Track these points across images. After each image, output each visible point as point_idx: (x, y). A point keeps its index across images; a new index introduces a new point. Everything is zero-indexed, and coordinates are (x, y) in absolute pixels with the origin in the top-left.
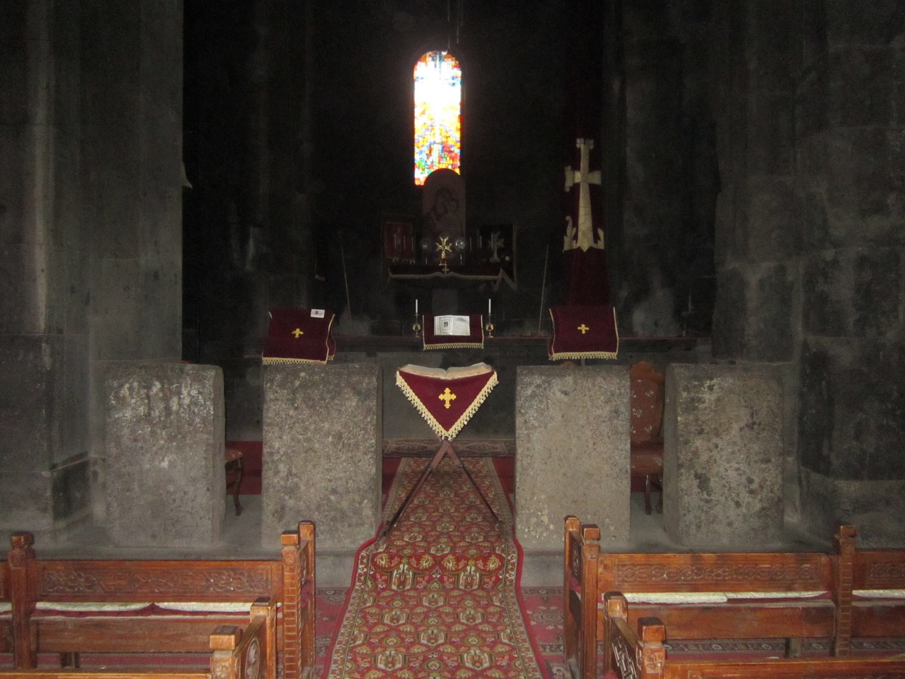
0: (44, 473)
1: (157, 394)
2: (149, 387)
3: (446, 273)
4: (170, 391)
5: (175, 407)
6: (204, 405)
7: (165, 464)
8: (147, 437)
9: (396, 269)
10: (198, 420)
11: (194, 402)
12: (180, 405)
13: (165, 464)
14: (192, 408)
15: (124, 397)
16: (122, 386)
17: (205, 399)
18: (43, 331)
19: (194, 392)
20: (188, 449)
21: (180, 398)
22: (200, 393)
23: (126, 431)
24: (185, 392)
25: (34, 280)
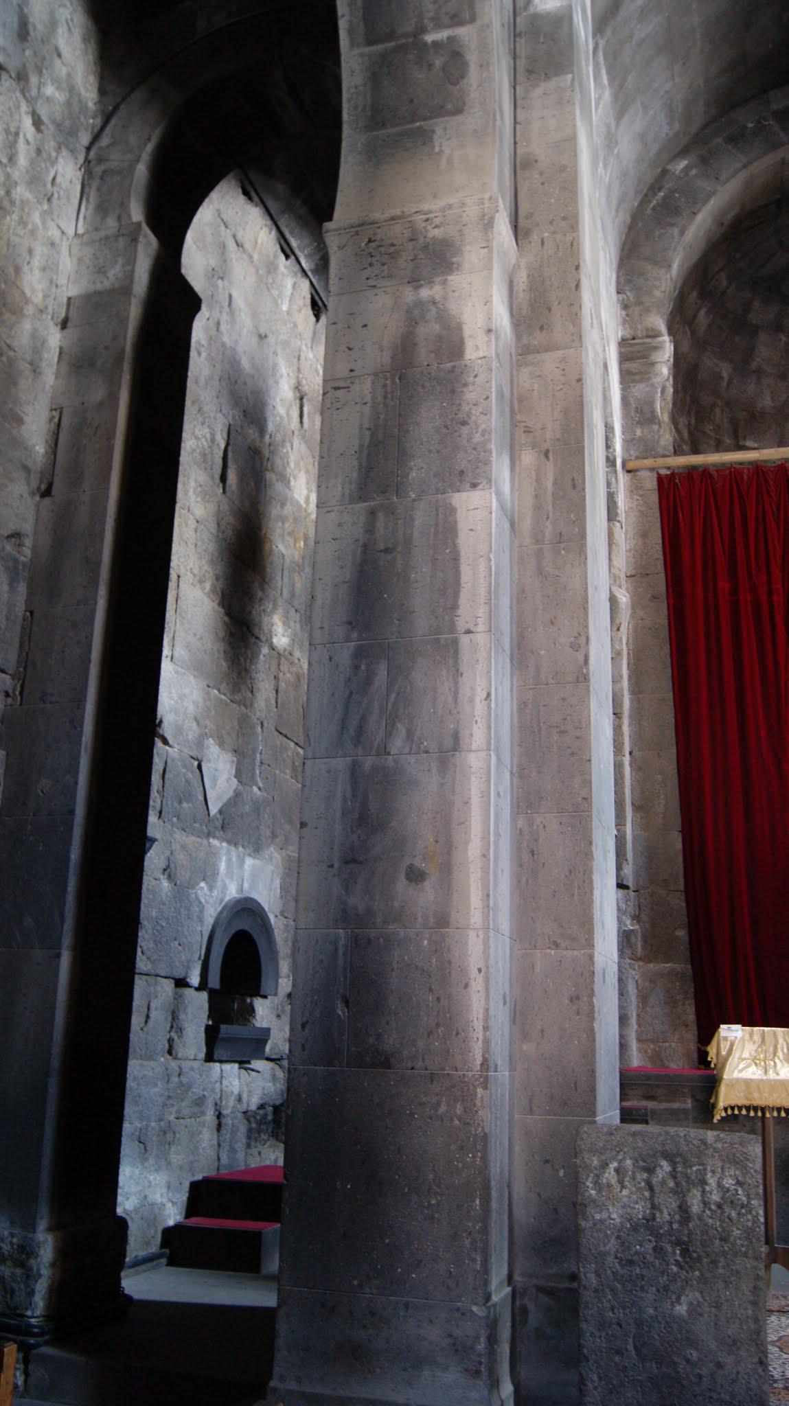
0: (475, 1308)
1: (663, 1183)
2: (650, 1170)
4: (688, 1177)
5: (696, 1208)
6: (748, 1207)
7: (682, 1309)
8: (650, 1258)
10: (736, 1232)
12: (705, 1204)
13: (682, 1309)
14: (727, 1209)
15: (609, 1186)
16: (605, 1165)
17: (748, 1196)
18: (479, 1068)
19: (728, 1182)
20: (720, 1285)
21: (704, 1191)
22: (739, 1183)
23: (612, 1245)
24: (712, 1181)
25: (466, 986)
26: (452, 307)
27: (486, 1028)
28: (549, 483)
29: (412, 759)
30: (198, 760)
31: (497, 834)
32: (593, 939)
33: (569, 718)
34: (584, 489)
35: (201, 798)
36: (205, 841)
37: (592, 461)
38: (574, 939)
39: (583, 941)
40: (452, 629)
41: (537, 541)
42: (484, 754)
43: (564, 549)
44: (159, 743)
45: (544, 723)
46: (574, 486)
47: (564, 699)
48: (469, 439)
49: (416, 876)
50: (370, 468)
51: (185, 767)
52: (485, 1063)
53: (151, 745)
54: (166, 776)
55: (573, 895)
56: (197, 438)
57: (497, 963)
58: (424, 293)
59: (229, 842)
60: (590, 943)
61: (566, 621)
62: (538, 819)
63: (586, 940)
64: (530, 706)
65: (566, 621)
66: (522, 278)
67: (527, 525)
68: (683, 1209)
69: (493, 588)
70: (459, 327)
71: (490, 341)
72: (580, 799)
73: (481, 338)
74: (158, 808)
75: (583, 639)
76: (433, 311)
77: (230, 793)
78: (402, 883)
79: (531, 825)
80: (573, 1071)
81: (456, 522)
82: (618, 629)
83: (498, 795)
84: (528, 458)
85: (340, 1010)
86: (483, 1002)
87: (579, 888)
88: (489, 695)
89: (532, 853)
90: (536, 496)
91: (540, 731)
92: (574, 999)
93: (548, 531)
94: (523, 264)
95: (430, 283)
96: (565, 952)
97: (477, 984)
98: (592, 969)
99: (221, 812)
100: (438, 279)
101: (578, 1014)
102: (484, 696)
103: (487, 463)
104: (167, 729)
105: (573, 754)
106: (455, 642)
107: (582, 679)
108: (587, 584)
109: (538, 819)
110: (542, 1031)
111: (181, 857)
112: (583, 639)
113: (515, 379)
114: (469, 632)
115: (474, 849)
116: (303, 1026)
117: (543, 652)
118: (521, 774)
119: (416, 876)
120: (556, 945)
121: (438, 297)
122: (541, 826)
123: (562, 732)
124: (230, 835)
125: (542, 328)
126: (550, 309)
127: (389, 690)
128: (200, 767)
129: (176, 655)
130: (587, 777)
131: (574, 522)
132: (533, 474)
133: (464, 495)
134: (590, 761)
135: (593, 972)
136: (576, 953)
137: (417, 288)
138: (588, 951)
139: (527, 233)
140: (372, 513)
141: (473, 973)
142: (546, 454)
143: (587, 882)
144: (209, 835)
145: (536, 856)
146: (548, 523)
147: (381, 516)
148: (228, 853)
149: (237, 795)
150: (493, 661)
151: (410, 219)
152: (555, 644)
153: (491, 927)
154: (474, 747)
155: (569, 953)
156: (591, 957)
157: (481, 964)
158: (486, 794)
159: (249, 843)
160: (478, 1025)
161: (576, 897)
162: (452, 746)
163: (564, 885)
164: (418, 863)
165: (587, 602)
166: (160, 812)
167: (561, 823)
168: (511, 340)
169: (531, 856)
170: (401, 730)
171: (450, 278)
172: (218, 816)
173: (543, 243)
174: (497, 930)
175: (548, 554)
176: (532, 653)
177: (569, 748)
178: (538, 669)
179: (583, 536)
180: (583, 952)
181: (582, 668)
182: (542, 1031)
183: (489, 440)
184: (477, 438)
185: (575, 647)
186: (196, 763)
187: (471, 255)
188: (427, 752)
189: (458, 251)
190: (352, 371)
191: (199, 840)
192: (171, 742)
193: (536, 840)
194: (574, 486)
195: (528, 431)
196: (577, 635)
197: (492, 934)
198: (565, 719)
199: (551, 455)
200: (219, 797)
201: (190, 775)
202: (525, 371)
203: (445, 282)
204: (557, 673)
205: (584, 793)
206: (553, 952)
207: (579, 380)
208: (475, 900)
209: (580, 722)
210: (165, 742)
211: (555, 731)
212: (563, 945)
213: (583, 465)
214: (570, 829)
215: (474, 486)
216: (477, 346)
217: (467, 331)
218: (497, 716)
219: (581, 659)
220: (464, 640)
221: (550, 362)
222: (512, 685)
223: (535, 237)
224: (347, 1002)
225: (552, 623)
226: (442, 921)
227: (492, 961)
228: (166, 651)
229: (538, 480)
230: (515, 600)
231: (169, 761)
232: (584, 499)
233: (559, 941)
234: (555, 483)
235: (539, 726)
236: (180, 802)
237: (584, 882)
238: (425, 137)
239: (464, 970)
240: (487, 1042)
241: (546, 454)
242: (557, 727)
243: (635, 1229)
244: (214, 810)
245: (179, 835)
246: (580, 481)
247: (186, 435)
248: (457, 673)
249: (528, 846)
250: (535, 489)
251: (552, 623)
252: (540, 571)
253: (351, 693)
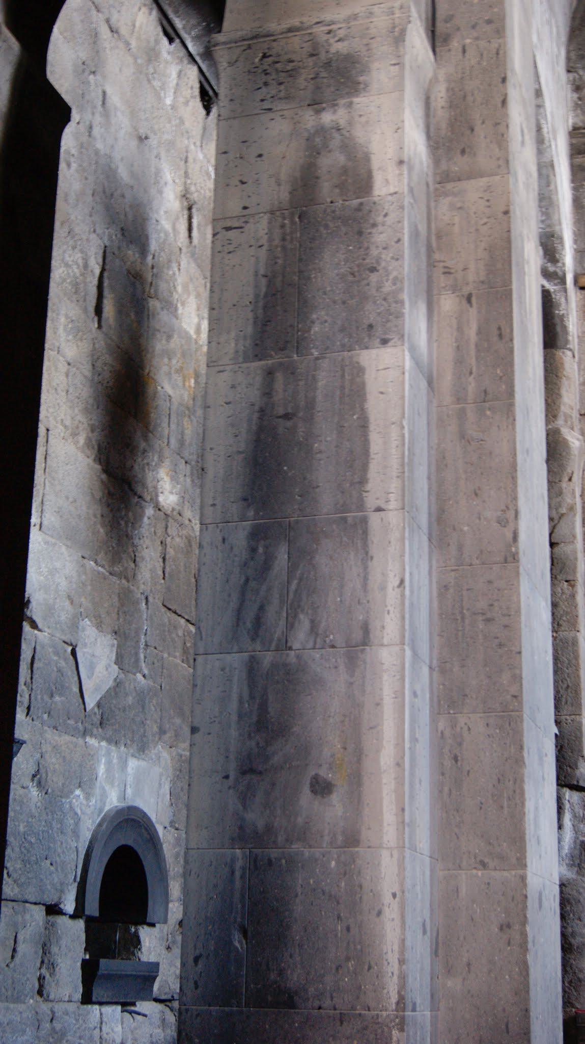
18: (394, 1007)
25: (379, 913)
26: (359, 134)
27: (402, 962)
28: (472, 332)
29: (317, 655)
30: (71, 645)
31: (414, 740)
32: (525, 858)
33: (496, 604)
34: (512, 340)
35: (76, 689)
36: (81, 741)
37: (522, 303)
38: (502, 858)
39: (514, 861)
40: (361, 506)
41: (458, 400)
42: (397, 649)
43: (489, 409)
44: (26, 627)
45: (468, 609)
46: (500, 336)
47: (490, 582)
48: (378, 289)
49: (321, 788)
50: (266, 322)
51: (57, 653)
52: (401, 1002)
53: (20, 628)
54: (35, 666)
55: (502, 807)
56: (67, 265)
57: (414, 886)
58: (327, 118)
59: (109, 741)
60: (521, 863)
61: (492, 493)
62: (462, 720)
63: (518, 859)
64: (451, 591)
65: (492, 493)
66: (440, 95)
67: (447, 381)
70: (367, 158)
71: (401, 174)
72: (509, 697)
73: (392, 171)
74: (26, 705)
75: (511, 514)
77: (110, 683)
78: (306, 796)
79: (453, 726)
80: (504, 1010)
81: (364, 384)
82: (570, 480)
83: (415, 694)
84: (448, 303)
85: (238, 941)
86: (398, 930)
87: (509, 799)
88: (402, 582)
89: (456, 759)
90: (458, 347)
91: (463, 618)
92: (505, 927)
93: (472, 388)
94: (441, 76)
96: (493, 873)
97: (391, 912)
98: (525, 892)
99: (99, 705)
100: (342, 102)
101: (509, 944)
103: (399, 315)
104: (35, 610)
105: (500, 645)
106: (364, 521)
107: (510, 559)
108: (515, 449)
109: (462, 720)
110: (469, 965)
111: (52, 761)
112: (511, 514)
113: (433, 212)
114: (379, 509)
115: (386, 757)
116: (196, 960)
117: (466, 528)
118: (442, 668)
119: (321, 788)
120: (484, 865)
121: (342, 123)
122: (466, 728)
123: (488, 620)
124: (110, 733)
125: (463, 152)
126: (472, 130)
127: (291, 572)
128: (74, 653)
129: (45, 523)
130: (517, 672)
131: (501, 377)
132: (454, 322)
133: (374, 352)
134: (520, 653)
135: (526, 897)
136: (506, 874)
137: (318, 112)
138: (520, 872)
139: (447, 39)
140: (270, 373)
141: (387, 898)
142: (469, 299)
143: (518, 792)
144: (85, 733)
145: (459, 764)
146: (471, 379)
147: (279, 377)
148: (108, 753)
149: (118, 684)
150: (407, 542)
151: (309, 31)
152: (480, 519)
153: (407, 845)
154: (385, 641)
155: (497, 874)
156: (523, 879)
157: (396, 888)
158: (399, 695)
159: (132, 741)
160: (393, 958)
161: (506, 810)
163: (493, 796)
164: (323, 773)
165: (516, 471)
166: (29, 708)
167: (487, 725)
168: (428, 167)
169: (454, 762)
170: (304, 621)
171: (356, 100)
172: (96, 710)
173: (464, 51)
174: (413, 848)
175: (471, 415)
176: (454, 529)
177: (497, 638)
178: (460, 548)
179: (511, 393)
180: (513, 872)
181: (511, 546)
182: (469, 965)
183: (401, 290)
184: (388, 287)
185: (502, 522)
186: (70, 648)
188: (333, 647)
189: (365, 70)
190: (245, 208)
191: (74, 739)
192: (40, 626)
193: (460, 744)
194: (500, 336)
195: (447, 272)
196: (504, 508)
197: (408, 853)
198: (492, 605)
199: (474, 300)
200: (96, 689)
201: (63, 664)
202: (445, 202)
203: (350, 104)
204: (481, 552)
205: (513, 690)
206: (480, 873)
207: (506, 213)
208: (389, 816)
209: (508, 608)
210: (34, 625)
211: (480, 618)
212: (491, 864)
213: (511, 312)
214: (498, 731)
215: (385, 342)
216: (387, 181)
217: (375, 163)
218: (412, 604)
219: (509, 536)
220: (375, 520)
221: (473, 190)
222: (431, 567)
223: (455, 44)
224: (244, 932)
225: (476, 495)
226: (352, 839)
227: (408, 883)
228: (34, 520)
229: (460, 329)
230: (433, 468)
231: (38, 648)
232: (511, 351)
233: (486, 860)
234: (479, 332)
235: (461, 613)
236: (52, 696)
237: (514, 792)
239: (377, 896)
240: (403, 978)
241: (469, 299)
242: (483, 614)
244: (91, 703)
245: (49, 734)
246: (508, 330)
247: (54, 263)
248: (367, 557)
249: (450, 751)
250: (457, 340)
251: (476, 495)
252: (462, 436)
253: (247, 580)
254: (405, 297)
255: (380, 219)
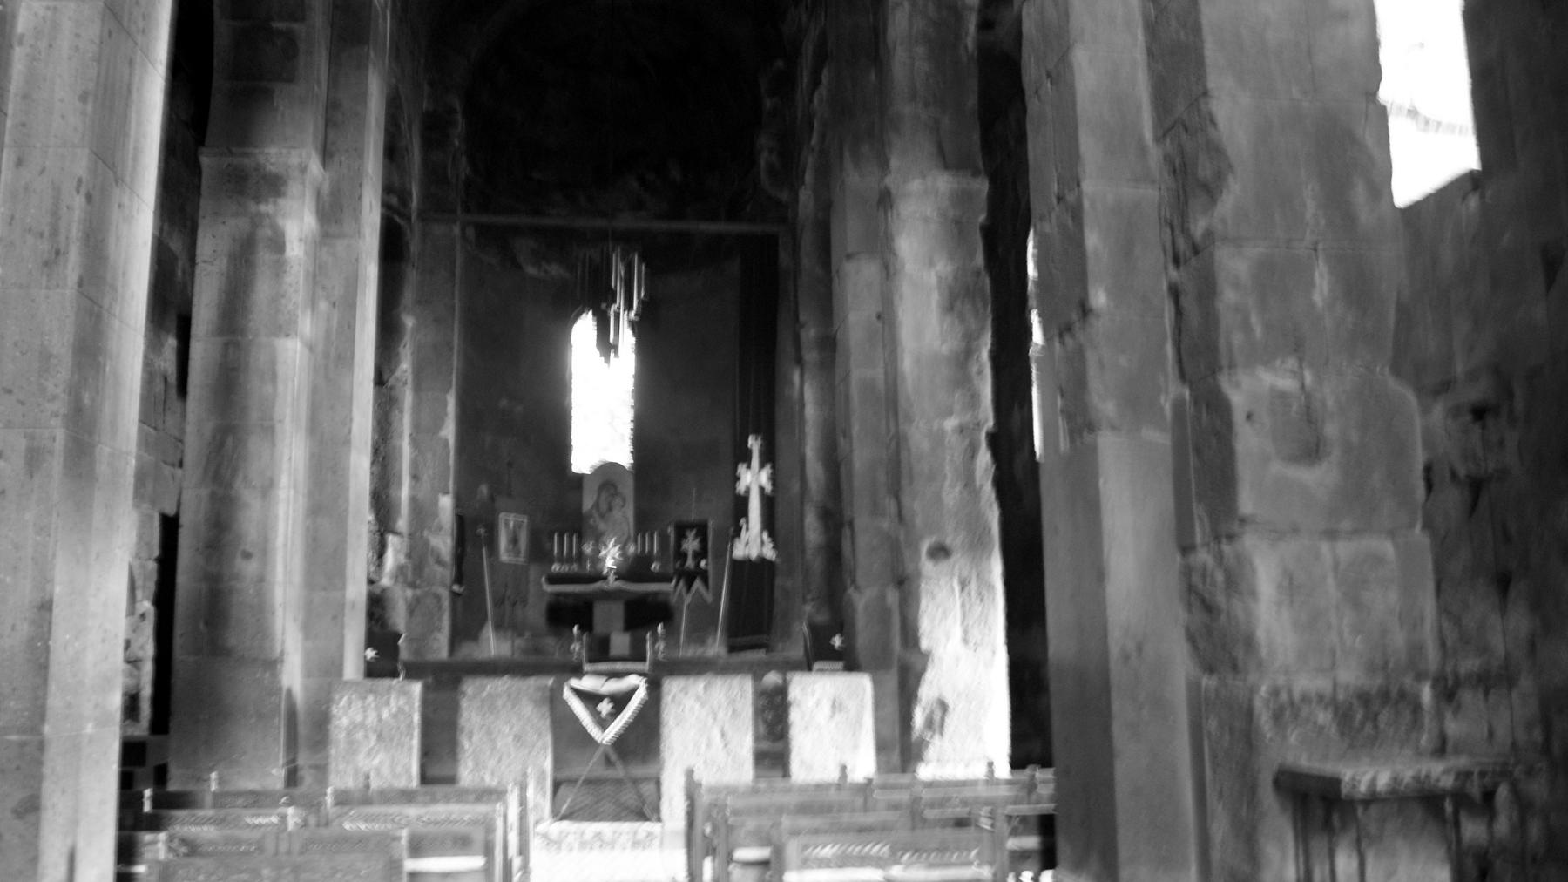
3: (612, 583)
9: (554, 579)
11: (400, 710)
26: (280, 222)
31: (293, 533)
40: (271, 419)
58: (263, 208)
66: (326, 188)
67: (320, 348)
68: (380, 720)
69: (296, 391)
76: (267, 221)
84: (323, 306)
88: (290, 458)
94: (327, 176)
95: (267, 202)
100: (271, 200)
102: (288, 458)
103: (296, 322)
114: (280, 421)
115: (280, 541)
118: (311, 494)
119: (247, 556)
125: (336, 222)
126: (342, 210)
137: (258, 203)
139: (332, 155)
142: (334, 304)
156: (344, 596)
162: (268, 488)
164: (248, 548)
184: (290, 307)
187: (293, 188)
189: (285, 183)
195: (324, 288)
199: (337, 304)
202: (325, 249)
207: (357, 260)
215: (287, 335)
221: (340, 245)
223: (336, 159)
226: (261, 579)
238: (268, 94)
243: (355, 727)
248: (273, 444)
254: (299, 312)
255: (288, 269)
